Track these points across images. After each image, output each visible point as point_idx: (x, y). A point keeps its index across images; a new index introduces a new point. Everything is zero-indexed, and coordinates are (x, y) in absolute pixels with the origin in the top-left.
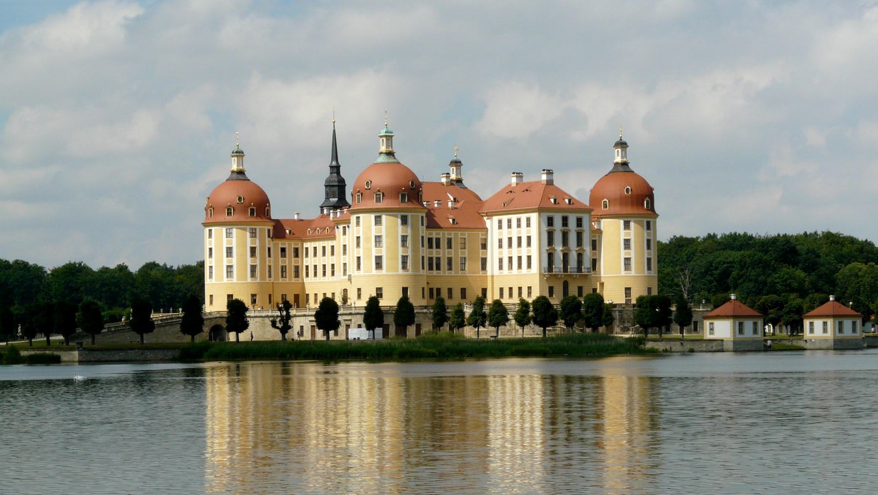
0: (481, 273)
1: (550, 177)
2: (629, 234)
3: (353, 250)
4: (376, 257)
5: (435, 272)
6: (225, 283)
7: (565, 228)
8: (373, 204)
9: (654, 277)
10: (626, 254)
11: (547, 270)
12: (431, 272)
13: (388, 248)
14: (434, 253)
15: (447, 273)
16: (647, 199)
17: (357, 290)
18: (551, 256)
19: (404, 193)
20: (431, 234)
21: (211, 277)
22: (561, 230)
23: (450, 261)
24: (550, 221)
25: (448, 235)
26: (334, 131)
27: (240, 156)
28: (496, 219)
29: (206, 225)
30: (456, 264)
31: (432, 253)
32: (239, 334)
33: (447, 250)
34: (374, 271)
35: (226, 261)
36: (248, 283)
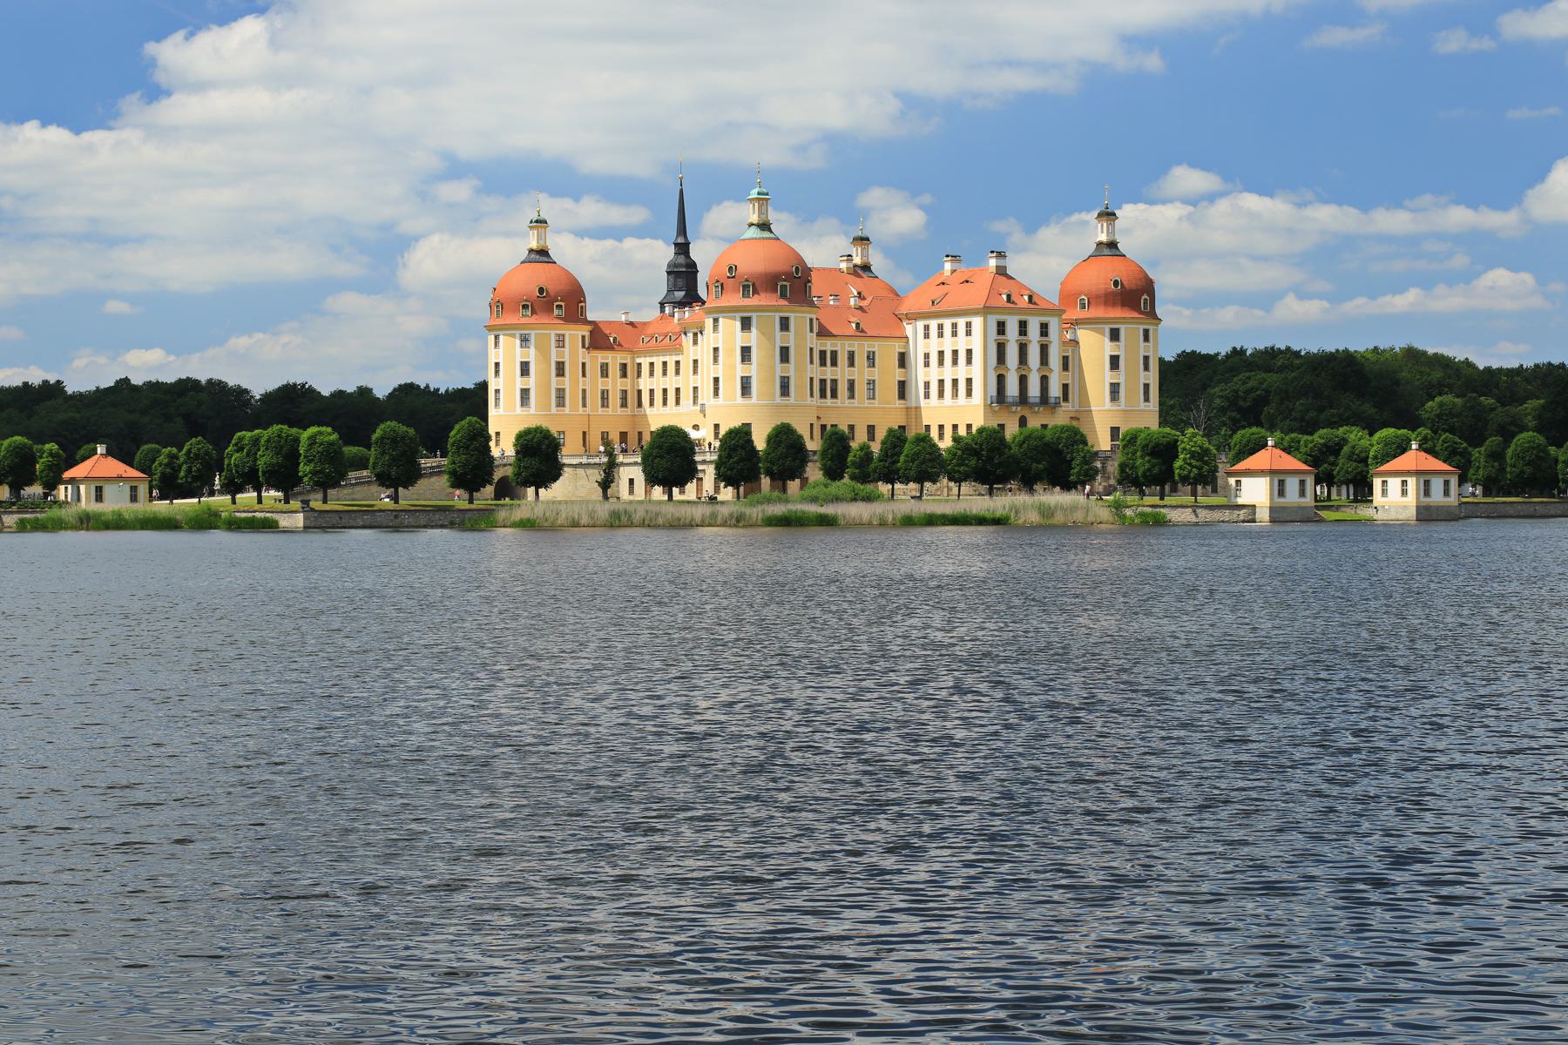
1: (1002, 262)
3: (708, 368)
5: (829, 401)
8: (736, 299)
12: (823, 400)
13: (758, 365)
14: (829, 373)
15: (847, 402)
16: (1145, 296)
17: (713, 427)
18: (1001, 379)
19: (784, 283)
20: (825, 345)
21: (497, 404)
26: (681, 191)
27: (541, 227)
28: (920, 324)
29: (490, 328)
30: (860, 389)
31: (824, 373)
33: (847, 369)
35: (520, 383)
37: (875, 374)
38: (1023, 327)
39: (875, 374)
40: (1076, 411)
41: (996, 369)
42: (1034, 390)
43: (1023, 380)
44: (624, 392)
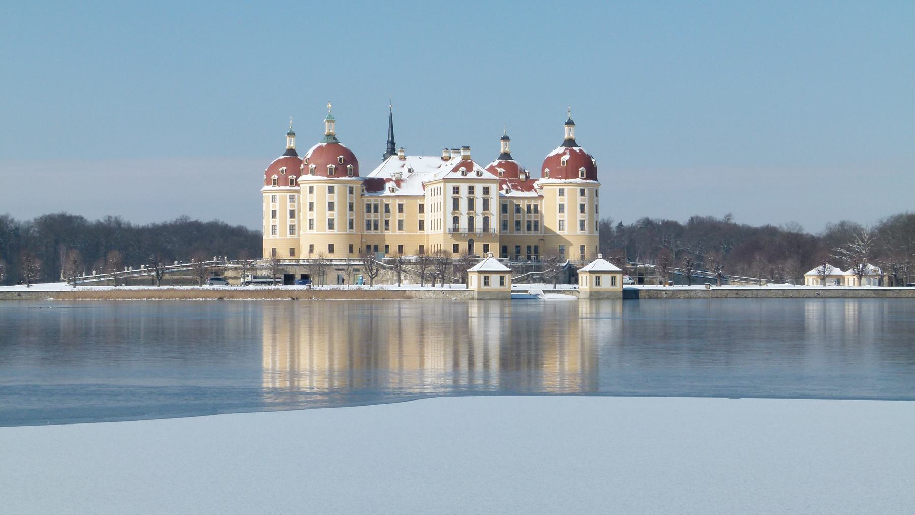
0: (419, 232)
2: (563, 200)
3: (306, 213)
5: (372, 232)
9: (597, 236)
10: (560, 216)
14: (372, 216)
18: (456, 220)
20: (370, 201)
23: (387, 222)
24: (456, 190)
26: (391, 114)
30: (382, 225)
32: (251, 280)
33: (366, 214)
34: (328, 231)
36: (287, 239)
37: (403, 216)
38: (471, 190)
39: (403, 216)
40: (544, 236)
41: (468, 214)
42: (479, 224)
43: (471, 220)
44: (529, 222)
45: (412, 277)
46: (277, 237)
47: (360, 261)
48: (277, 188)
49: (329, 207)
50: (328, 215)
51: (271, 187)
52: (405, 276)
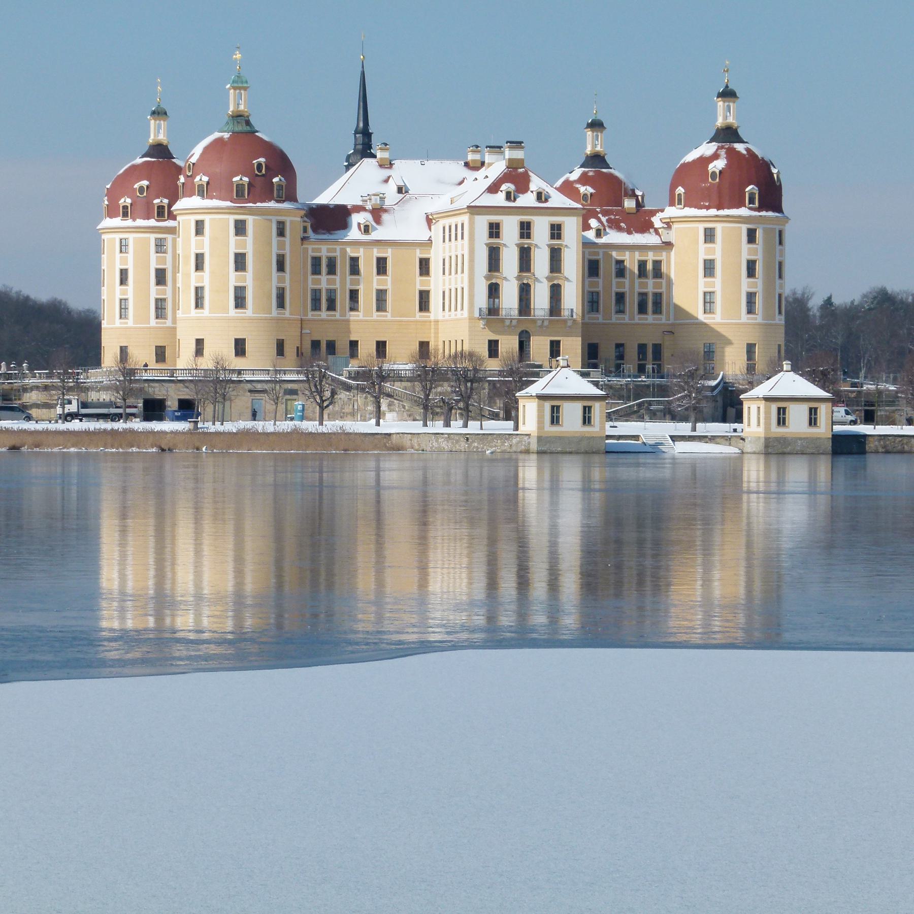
0: (419, 316)
2: (713, 251)
3: (188, 275)
4: (236, 288)
5: (324, 314)
6: (154, 328)
7: (494, 240)
11: (485, 311)
14: (324, 282)
18: (494, 290)
20: (319, 250)
22: (517, 245)
23: (354, 295)
24: (494, 230)
25: (328, 252)
26: (363, 74)
30: (343, 300)
31: (319, 282)
32: (76, 410)
33: (310, 278)
34: (233, 312)
36: (150, 328)
37: (387, 282)
38: (525, 229)
40: (673, 325)
41: (519, 278)
42: (541, 300)
43: (525, 291)
44: (643, 296)
45: (404, 407)
46: (130, 322)
47: (298, 372)
48: (129, 223)
49: (236, 262)
50: (233, 279)
51: (117, 222)
52: (390, 405)
